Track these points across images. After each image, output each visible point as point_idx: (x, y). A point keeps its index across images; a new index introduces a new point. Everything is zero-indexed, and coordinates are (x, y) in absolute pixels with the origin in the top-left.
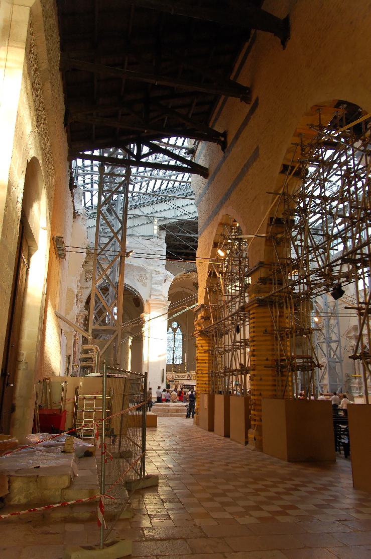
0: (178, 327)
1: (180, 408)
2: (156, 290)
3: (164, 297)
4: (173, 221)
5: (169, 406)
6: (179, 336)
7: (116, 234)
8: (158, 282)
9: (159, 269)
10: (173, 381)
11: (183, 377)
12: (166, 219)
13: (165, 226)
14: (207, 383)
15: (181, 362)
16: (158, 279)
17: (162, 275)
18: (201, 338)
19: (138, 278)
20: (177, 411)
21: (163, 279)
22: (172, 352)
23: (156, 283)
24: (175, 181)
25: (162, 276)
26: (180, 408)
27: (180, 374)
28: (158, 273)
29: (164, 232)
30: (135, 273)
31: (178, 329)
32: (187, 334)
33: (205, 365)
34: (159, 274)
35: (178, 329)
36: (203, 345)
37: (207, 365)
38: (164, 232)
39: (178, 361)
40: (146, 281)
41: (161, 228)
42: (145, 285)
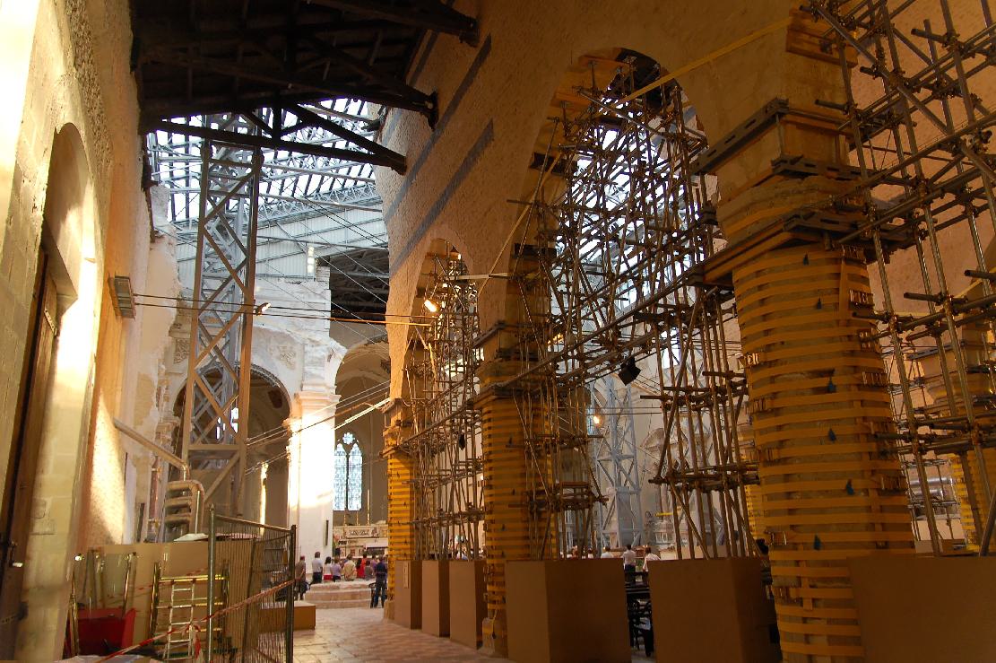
0: (354, 442)
1: (358, 590)
2: (313, 376)
4: (344, 249)
5: (338, 588)
6: (357, 459)
7: (234, 273)
8: (317, 360)
9: (317, 338)
10: (345, 543)
11: (363, 532)
12: (329, 245)
13: (328, 258)
14: (408, 540)
15: (360, 506)
17: (324, 348)
18: (396, 461)
19: (277, 353)
20: (354, 596)
21: (326, 354)
22: (344, 488)
23: (312, 363)
24: (346, 178)
25: (323, 351)
26: (358, 590)
27: (358, 528)
28: (315, 343)
29: (326, 271)
30: (273, 344)
31: (355, 445)
33: (404, 508)
34: (318, 345)
35: (355, 445)
36: (400, 472)
37: (408, 508)
38: (326, 271)
39: (356, 505)
40: (293, 360)
41: (322, 262)
42: (291, 366)
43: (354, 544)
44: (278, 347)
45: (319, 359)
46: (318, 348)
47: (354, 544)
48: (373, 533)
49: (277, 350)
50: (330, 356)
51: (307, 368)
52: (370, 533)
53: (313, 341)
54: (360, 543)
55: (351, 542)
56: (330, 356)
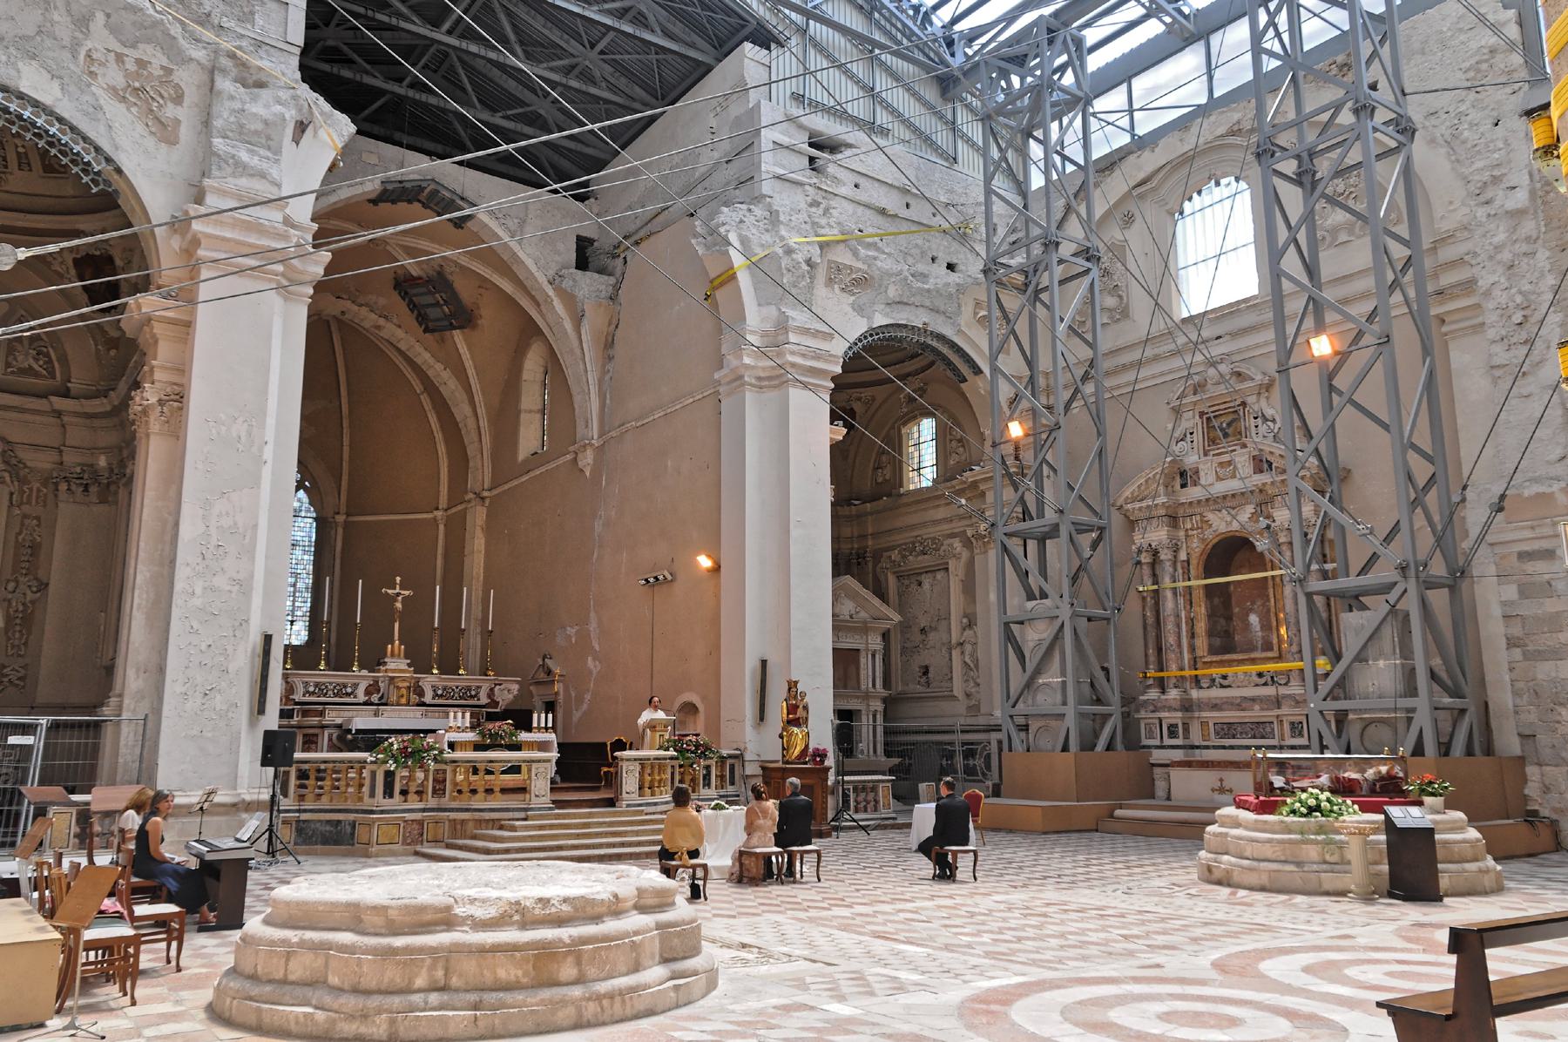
1: (565, 933)
2: (241, 168)
3: (288, 221)
5: (445, 919)
8: (260, 126)
9: (264, 62)
11: (340, 691)
16: (257, 109)
19: (114, 76)
21: (291, 115)
25: (279, 102)
26: (565, 933)
32: (341, 518)
40: (170, 111)
42: (166, 133)
43: (315, 720)
44: (120, 58)
45: (266, 123)
46: (264, 93)
47: (315, 720)
48: (368, 692)
49: (112, 64)
50: (301, 127)
51: (218, 142)
52: (361, 692)
53: (244, 65)
54: (333, 717)
55: (305, 713)
56: (301, 127)
